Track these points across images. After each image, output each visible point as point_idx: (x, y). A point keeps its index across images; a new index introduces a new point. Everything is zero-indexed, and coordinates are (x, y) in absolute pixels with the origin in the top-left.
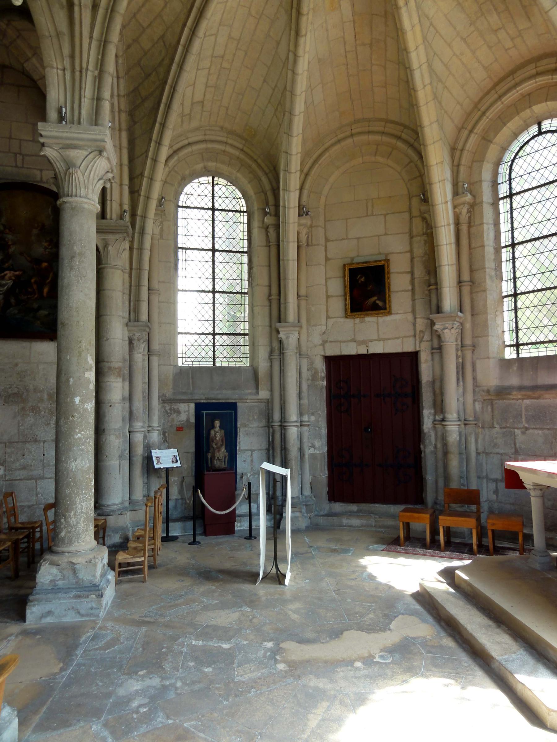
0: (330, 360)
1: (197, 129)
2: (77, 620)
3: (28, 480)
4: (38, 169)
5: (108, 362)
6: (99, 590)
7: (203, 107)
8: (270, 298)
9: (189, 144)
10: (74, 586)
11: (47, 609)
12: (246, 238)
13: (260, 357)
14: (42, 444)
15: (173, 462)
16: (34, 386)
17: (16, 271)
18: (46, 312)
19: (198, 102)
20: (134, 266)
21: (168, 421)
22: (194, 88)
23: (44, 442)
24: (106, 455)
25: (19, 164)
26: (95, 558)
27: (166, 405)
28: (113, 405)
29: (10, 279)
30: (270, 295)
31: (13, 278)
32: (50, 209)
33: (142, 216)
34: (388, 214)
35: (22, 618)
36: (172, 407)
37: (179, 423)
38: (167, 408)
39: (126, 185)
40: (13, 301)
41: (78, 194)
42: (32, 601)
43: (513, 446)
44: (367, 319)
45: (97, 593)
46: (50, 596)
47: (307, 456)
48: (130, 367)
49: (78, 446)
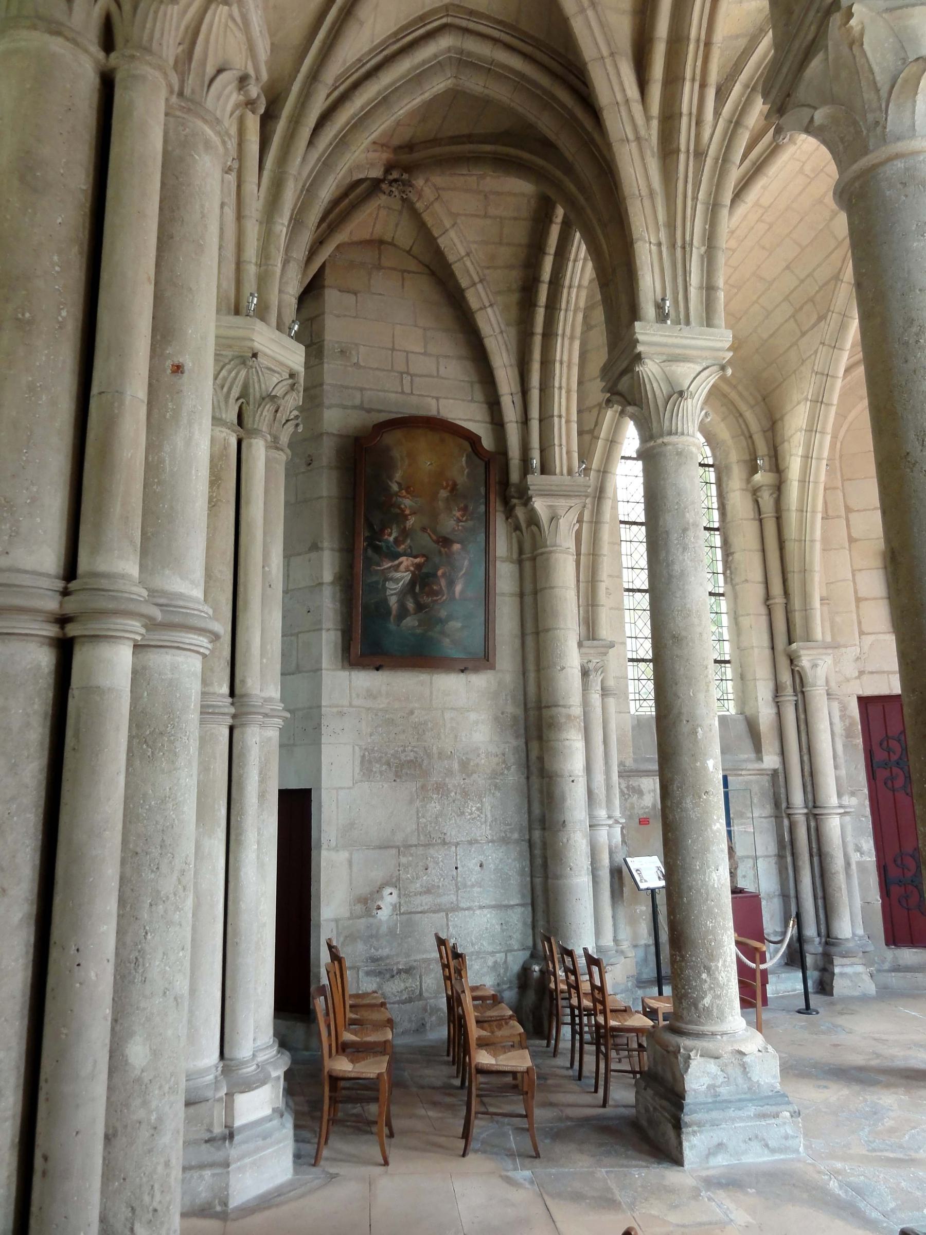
0: (865, 702)
2: (765, 1159)
3: (434, 912)
4: (433, 397)
5: (564, 706)
8: (768, 603)
10: (748, 1096)
11: (716, 1141)
12: (715, 506)
13: (760, 699)
14: (453, 848)
16: (438, 748)
17: (415, 557)
21: (626, 808)
24: (570, 866)
25: (407, 389)
28: (576, 779)
29: (407, 570)
30: (768, 597)
31: (412, 569)
32: (464, 459)
33: (599, 471)
35: (675, 1158)
36: (630, 783)
37: (642, 811)
40: (411, 605)
41: (686, 432)
45: (790, 1108)
47: (854, 866)
49: (718, 845)
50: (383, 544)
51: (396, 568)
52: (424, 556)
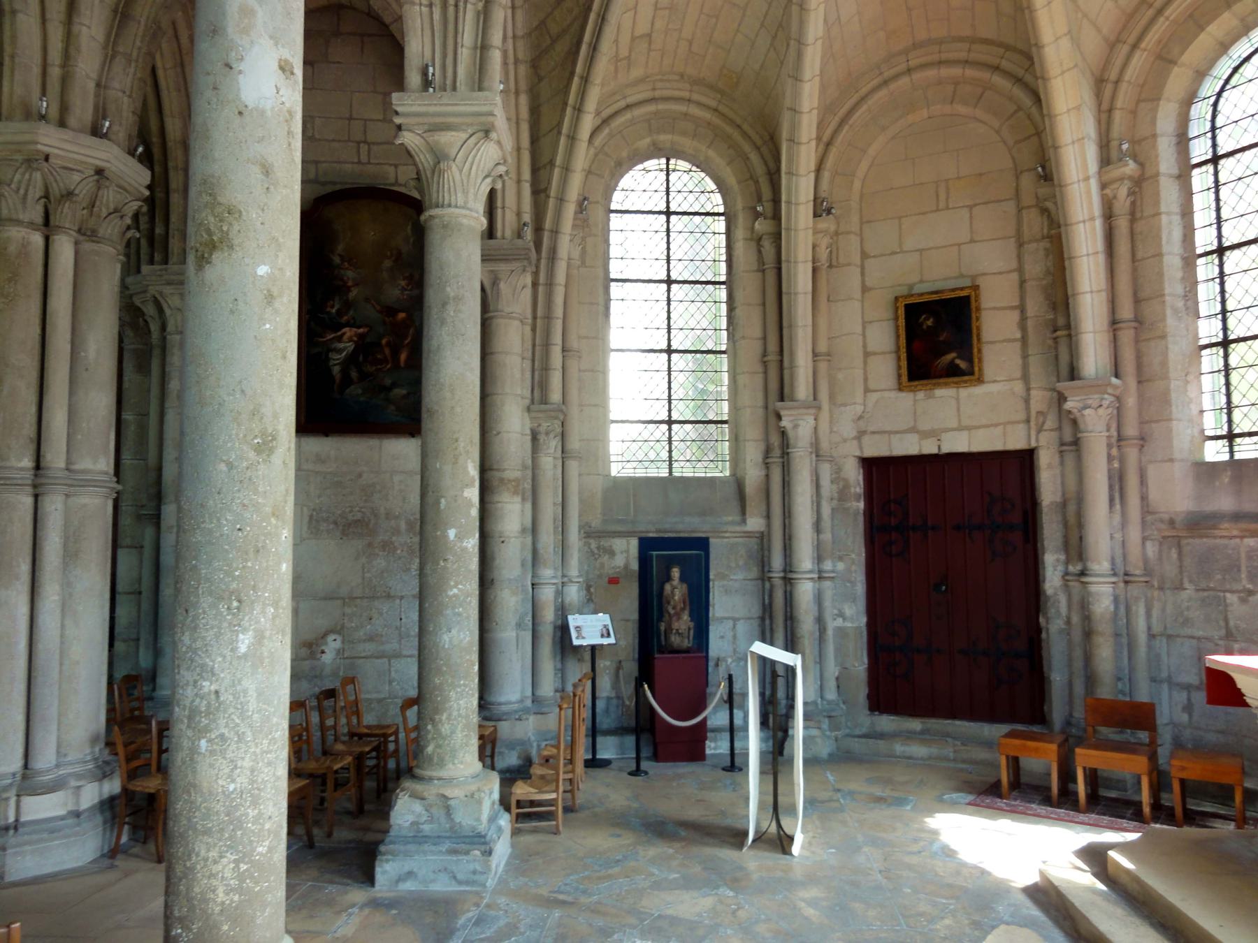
0: (871, 465)
1: (642, 80)
2: (450, 889)
3: (377, 658)
4: (391, 165)
5: (498, 470)
6: (485, 843)
7: (650, 44)
8: (766, 359)
9: (628, 107)
10: (448, 834)
11: (406, 869)
12: (724, 258)
13: (748, 460)
15: (602, 636)
16: (385, 509)
17: (359, 327)
18: (404, 392)
19: (641, 37)
20: (539, 313)
22: (636, 12)
23: (402, 598)
25: (364, 158)
26: (479, 790)
27: (592, 541)
29: (350, 340)
30: (765, 354)
31: (355, 339)
32: (409, 227)
33: (552, 231)
34: (976, 205)
35: (369, 878)
37: (613, 571)
38: (594, 545)
39: (526, 181)
40: (354, 374)
41: (453, 204)
42: (384, 854)
43: (1222, 623)
44: (939, 392)
45: (483, 848)
46: (411, 847)
47: (830, 632)
48: (534, 478)
49: (454, 608)
50: (325, 316)
51: (340, 339)
52: (366, 326)
